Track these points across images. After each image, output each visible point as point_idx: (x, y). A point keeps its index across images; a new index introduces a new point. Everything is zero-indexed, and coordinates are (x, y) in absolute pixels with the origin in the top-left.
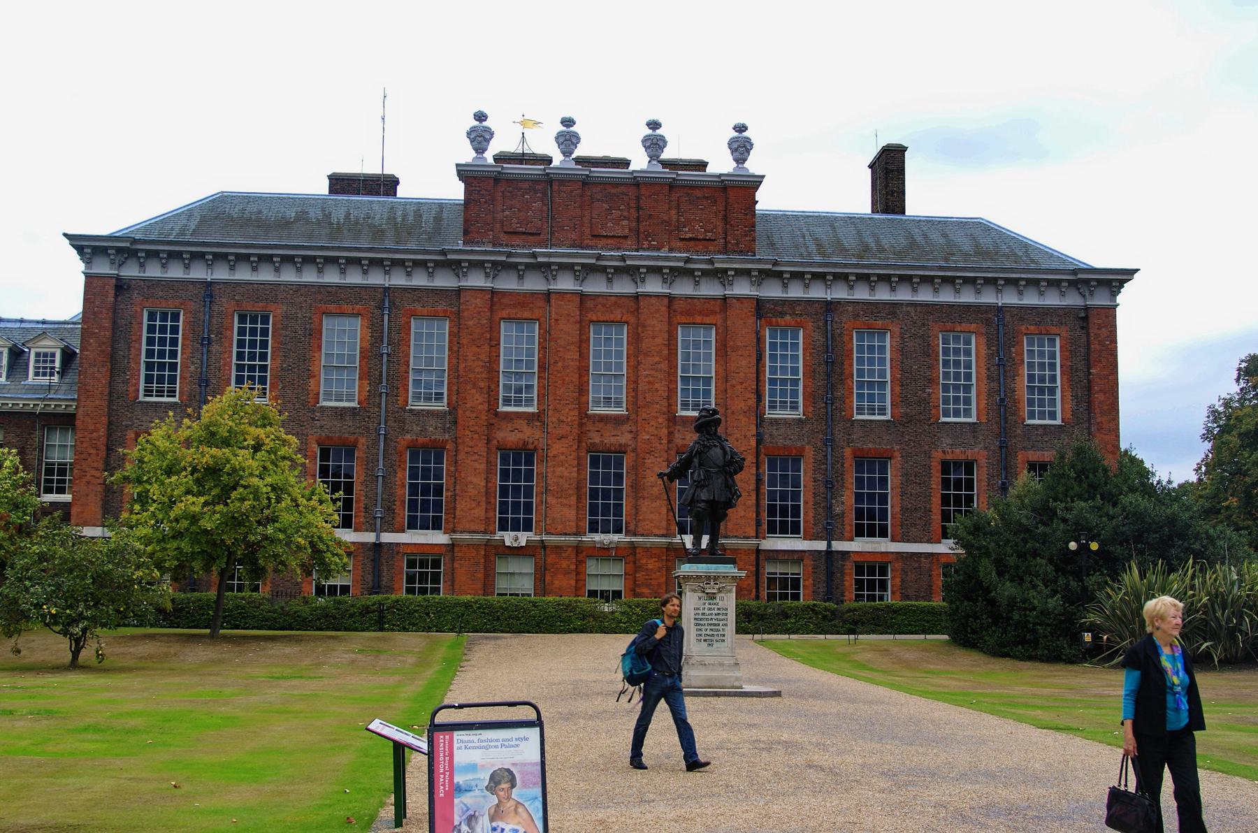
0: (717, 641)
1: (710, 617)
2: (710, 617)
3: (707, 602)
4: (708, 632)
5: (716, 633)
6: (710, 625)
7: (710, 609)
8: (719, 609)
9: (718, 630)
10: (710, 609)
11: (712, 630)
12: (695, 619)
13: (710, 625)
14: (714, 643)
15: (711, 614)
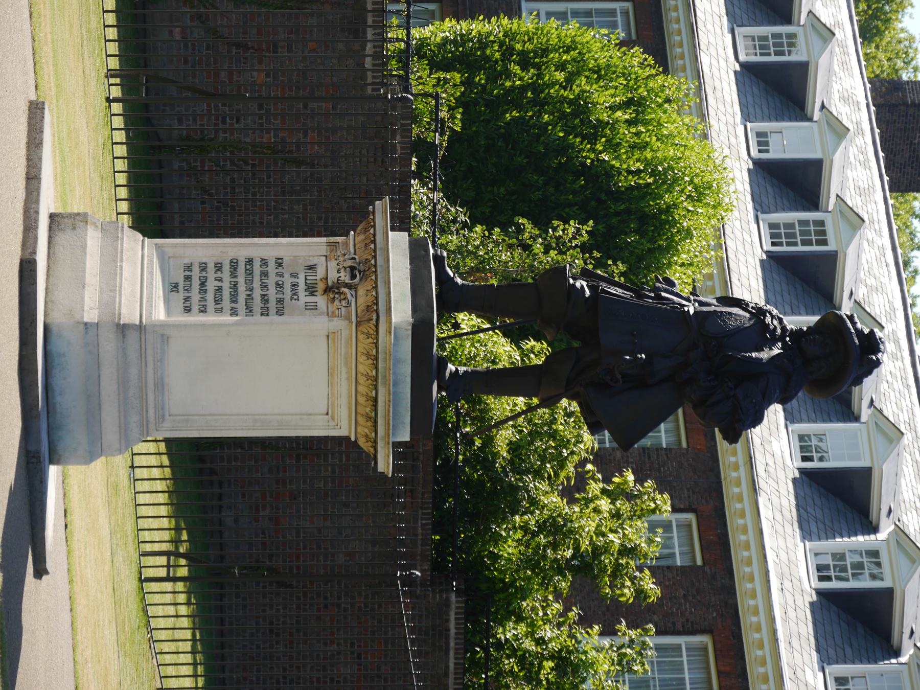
0: (187, 299)
1: (256, 284)
2: (256, 284)
3: (301, 281)
4: (211, 285)
5: (210, 296)
6: (235, 287)
7: (279, 286)
8: (280, 301)
9: (217, 301)
10: (279, 286)
11: (220, 289)
12: (250, 261)
13: (235, 287)
14: (182, 295)
15: (264, 287)
